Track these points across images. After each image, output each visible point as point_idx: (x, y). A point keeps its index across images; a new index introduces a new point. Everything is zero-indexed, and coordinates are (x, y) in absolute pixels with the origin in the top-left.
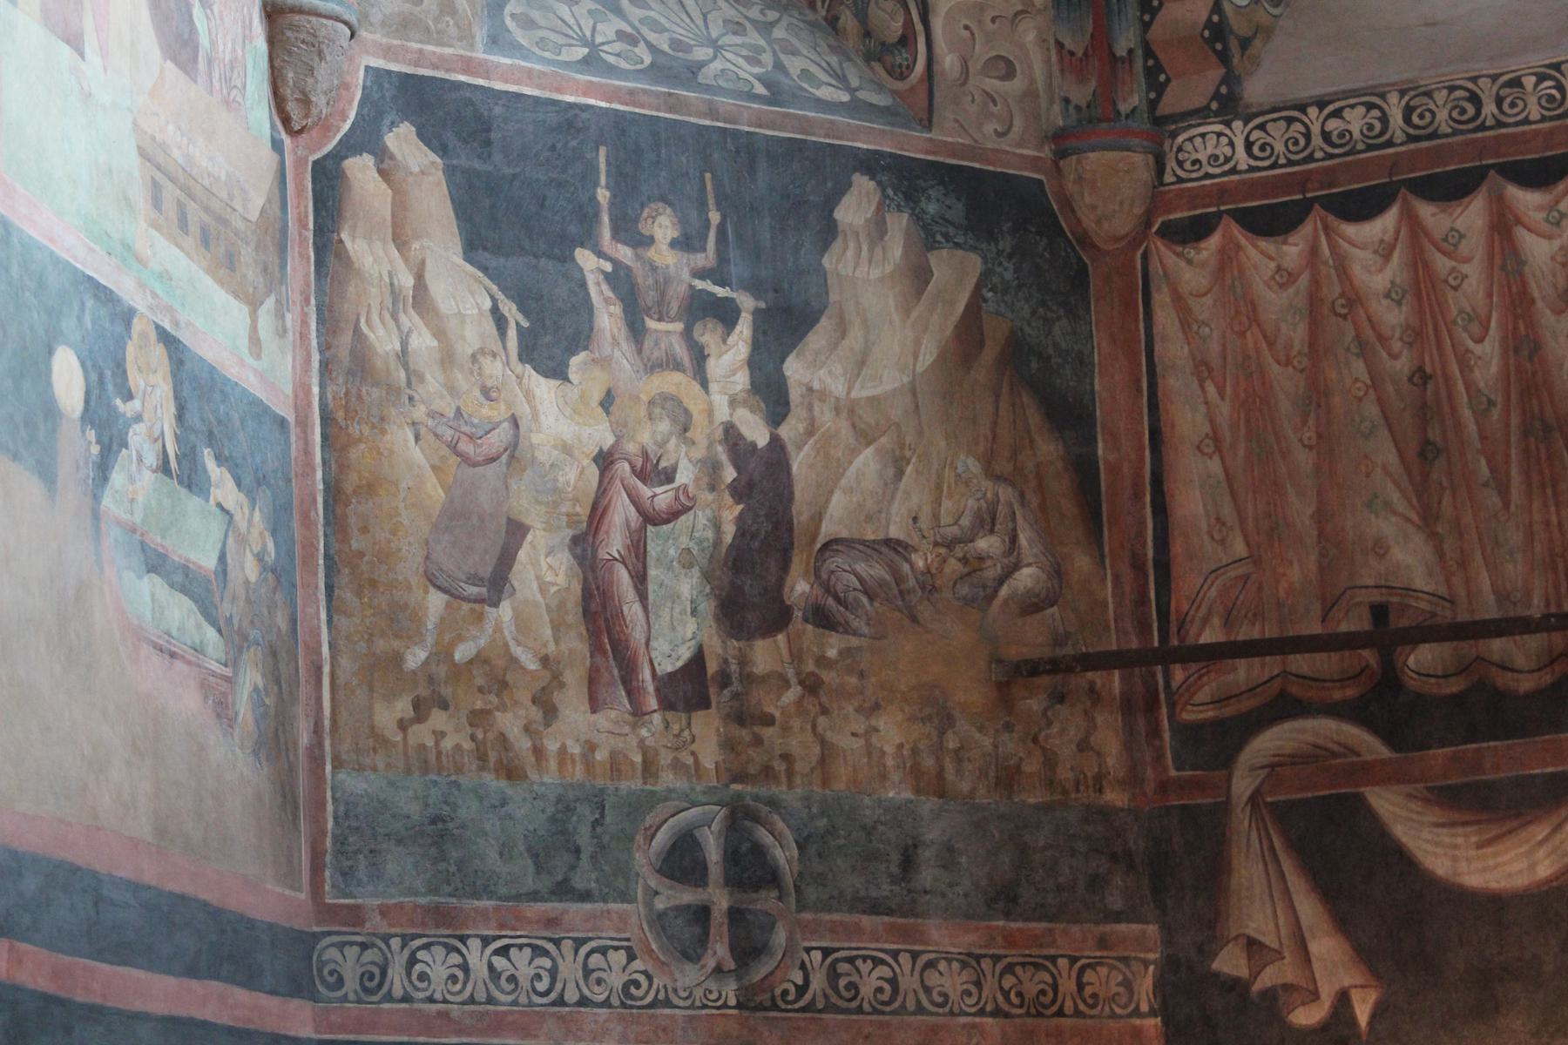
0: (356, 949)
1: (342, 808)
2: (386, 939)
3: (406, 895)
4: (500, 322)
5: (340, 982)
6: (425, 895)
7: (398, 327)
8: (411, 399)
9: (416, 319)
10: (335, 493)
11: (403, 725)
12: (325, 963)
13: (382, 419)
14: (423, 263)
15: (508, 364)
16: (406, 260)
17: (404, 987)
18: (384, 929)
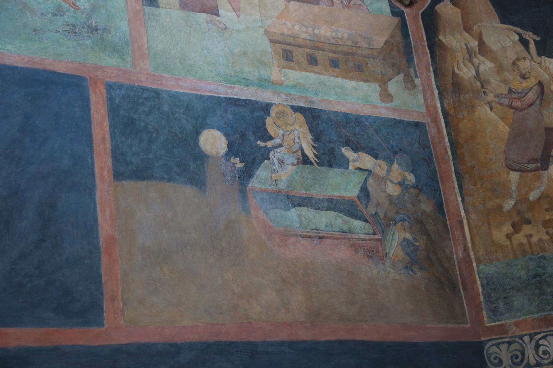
0: (506, 345)
1: (485, 281)
2: (521, 337)
3: (527, 315)
4: (525, 43)
5: (501, 362)
6: (537, 313)
7: (473, 65)
8: (485, 93)
9: (481, 58)
10: (454, 145)
11: (509, 237)
12: (491, 354)
13: (472, 107)
14: (481, 34)
15: (532, 59)
16: (472, 35)
17: (535, 359)
18: (519, 333)
